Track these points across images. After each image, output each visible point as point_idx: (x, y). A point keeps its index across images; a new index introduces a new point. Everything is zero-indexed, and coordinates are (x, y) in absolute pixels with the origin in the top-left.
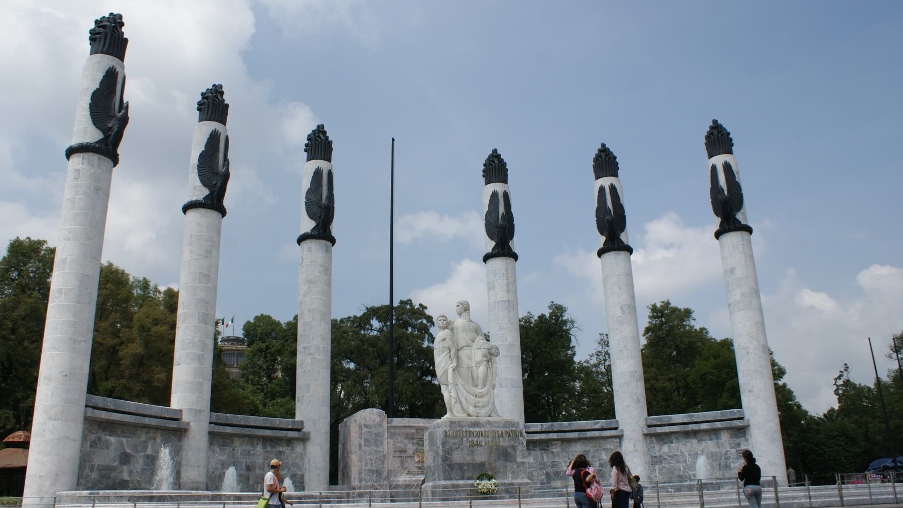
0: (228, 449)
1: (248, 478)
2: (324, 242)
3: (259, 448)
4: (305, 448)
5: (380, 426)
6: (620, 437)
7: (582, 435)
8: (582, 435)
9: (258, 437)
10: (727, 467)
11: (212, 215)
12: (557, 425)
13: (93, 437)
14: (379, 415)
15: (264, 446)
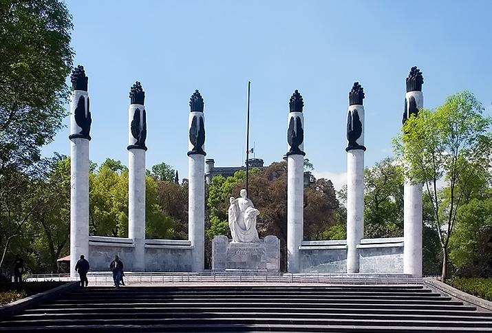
0: (154, 255)
1: (164, 266)
2: (199, 155)
3: (169, 254)
4: (192, 253)
5: (225, 243)
6: (347, 249)
7: (327, 247)
8: (327, 247)
9: (169, 249)
10: (393, 266)
11: (141, 151)
12: (318, 242)
13: (93, 252)
14: (224, 238)
15: (172, 253)
